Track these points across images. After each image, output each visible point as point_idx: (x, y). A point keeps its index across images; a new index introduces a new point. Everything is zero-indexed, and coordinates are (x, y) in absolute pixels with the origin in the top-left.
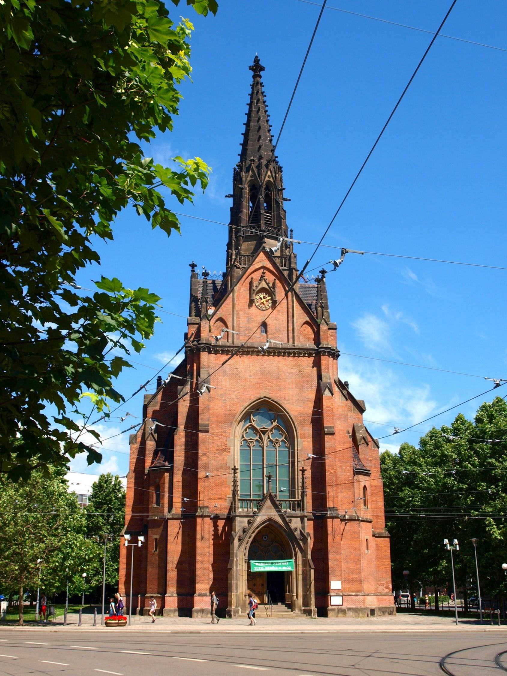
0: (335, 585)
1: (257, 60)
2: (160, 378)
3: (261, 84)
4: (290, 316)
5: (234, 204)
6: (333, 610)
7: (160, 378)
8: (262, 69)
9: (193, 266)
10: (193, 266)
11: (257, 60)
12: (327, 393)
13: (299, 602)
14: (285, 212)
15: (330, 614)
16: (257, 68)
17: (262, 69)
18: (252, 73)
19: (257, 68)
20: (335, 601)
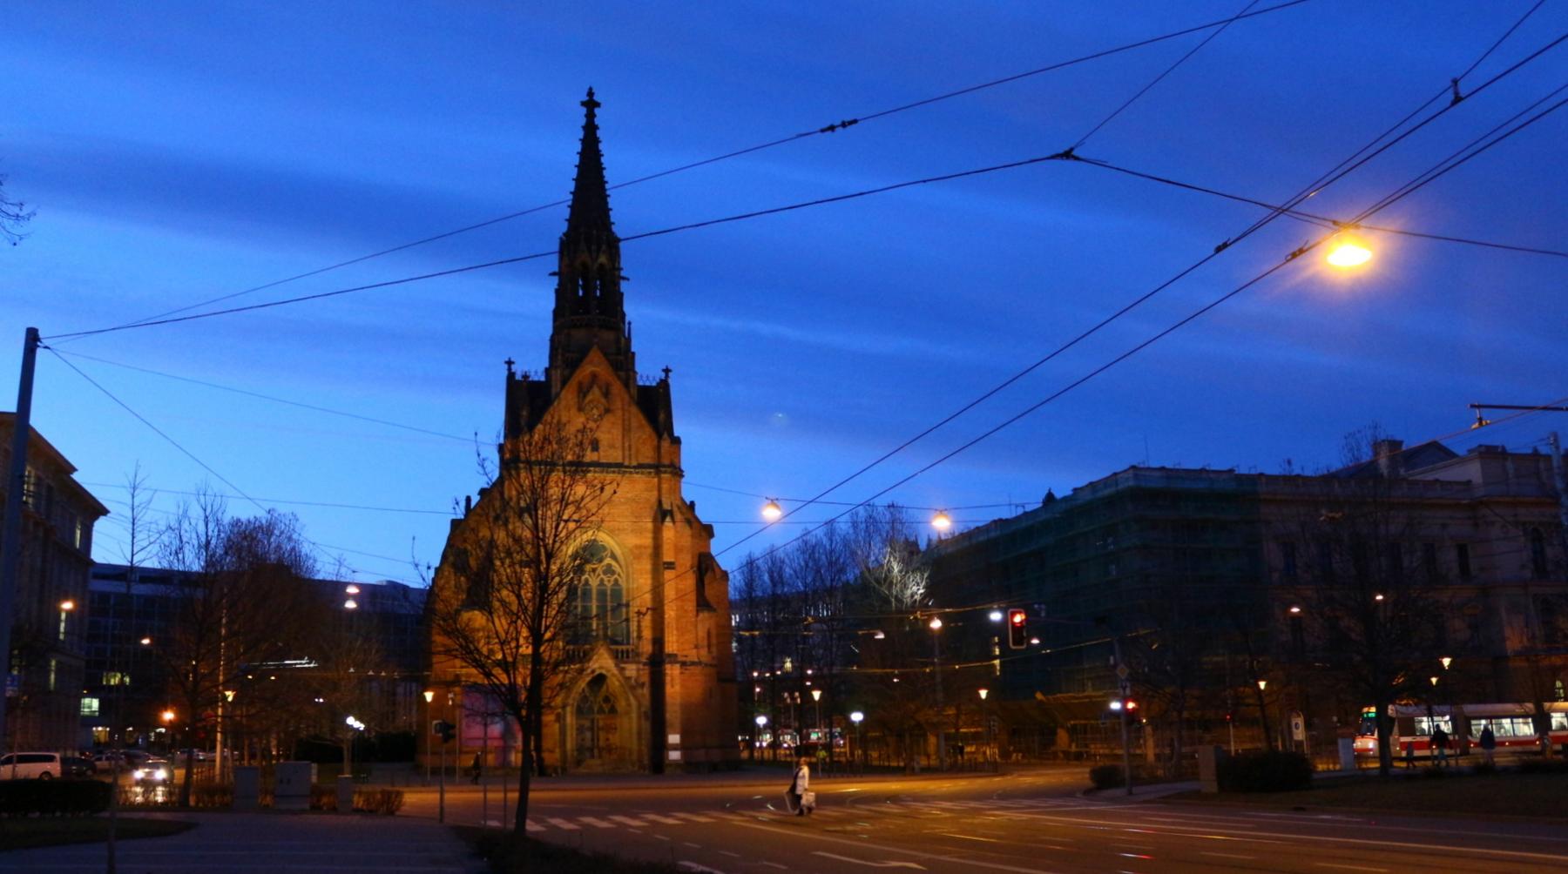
0: (674, 739)
1: (591, 94)
2: (468, 499)
3: (596, 128)
4: (626, 430)
5: (560, 284)
7: (468, 499)
8: (598, 105)
9: (510, 363)
10: (510, 363)
11: (591, 94)
12: (668, 522)
13: (635, 757)
14: (622, 294)
16: (591, 104)
17: (598, 105)
18: (584, 110)
19: (591, 104)
20: (675, 755)
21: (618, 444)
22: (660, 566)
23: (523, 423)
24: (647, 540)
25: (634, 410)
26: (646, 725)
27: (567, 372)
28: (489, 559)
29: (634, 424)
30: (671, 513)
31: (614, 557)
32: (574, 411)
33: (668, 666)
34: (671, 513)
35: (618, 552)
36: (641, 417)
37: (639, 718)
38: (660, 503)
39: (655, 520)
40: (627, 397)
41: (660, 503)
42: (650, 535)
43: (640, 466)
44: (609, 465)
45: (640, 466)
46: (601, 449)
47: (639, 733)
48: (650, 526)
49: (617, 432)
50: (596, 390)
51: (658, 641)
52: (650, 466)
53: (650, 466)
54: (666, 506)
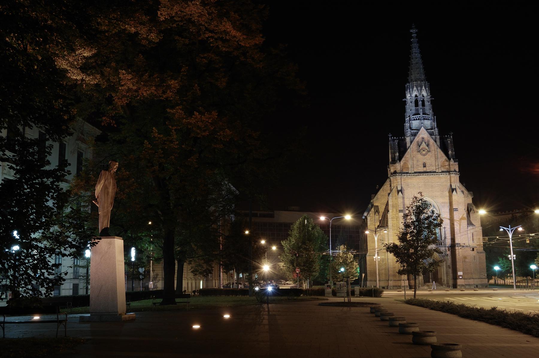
4: (436, 159)
6: (459, 285)
13: (445, 282)
15: (458, 287)
21: (434, 164)
22: (452, 210)
23: (396, 158)
24: (447, 200)
25: (439, 150)
26: (450, 271)
27: (412, 138)
28: (387, 210)
29: (439, 156)
30: (455, 189)
31: (434, 207)
32: (415, 153)
33: (457, 248)
34: (455, 189)
35: (435, 205)
36: (442, 153)
37: (447, 268)
38: (451, 185)
39: (449, 192)
40: (436, 145)
41: (451, 185)
42: (448, 198)
43: (443, 172)
44: (430, 172)
45: (443, 172)
46: (427, 166)
47: (447, 273)
48: (448, 194)
49: (433, 159)
50: (423, 143)
51: (453, 239)
52: (446, 172)
53: (446, 172)
54: (453, 187)
